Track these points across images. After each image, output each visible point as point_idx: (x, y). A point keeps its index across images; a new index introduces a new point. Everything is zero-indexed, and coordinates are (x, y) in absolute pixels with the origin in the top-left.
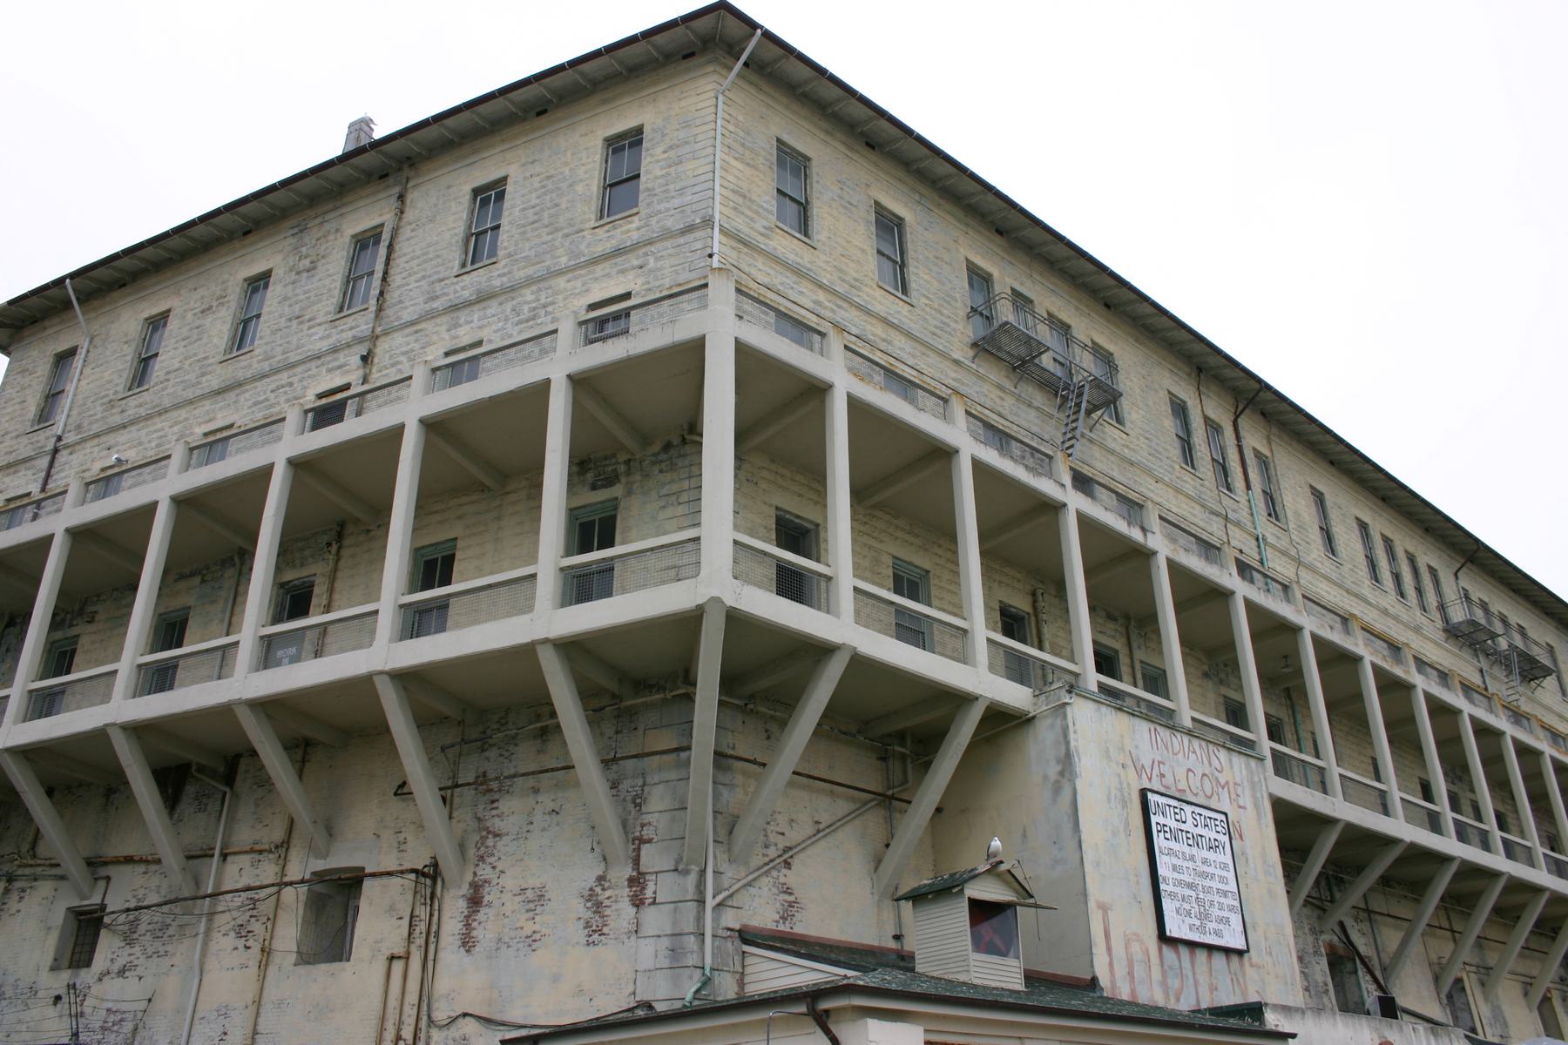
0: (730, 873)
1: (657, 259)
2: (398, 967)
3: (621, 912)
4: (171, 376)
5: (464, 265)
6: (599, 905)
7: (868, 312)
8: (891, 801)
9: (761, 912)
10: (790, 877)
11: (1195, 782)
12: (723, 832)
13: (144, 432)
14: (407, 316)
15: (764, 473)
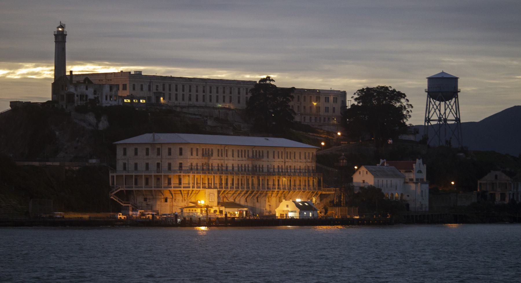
3: (184, 201)
9: (190, 201)
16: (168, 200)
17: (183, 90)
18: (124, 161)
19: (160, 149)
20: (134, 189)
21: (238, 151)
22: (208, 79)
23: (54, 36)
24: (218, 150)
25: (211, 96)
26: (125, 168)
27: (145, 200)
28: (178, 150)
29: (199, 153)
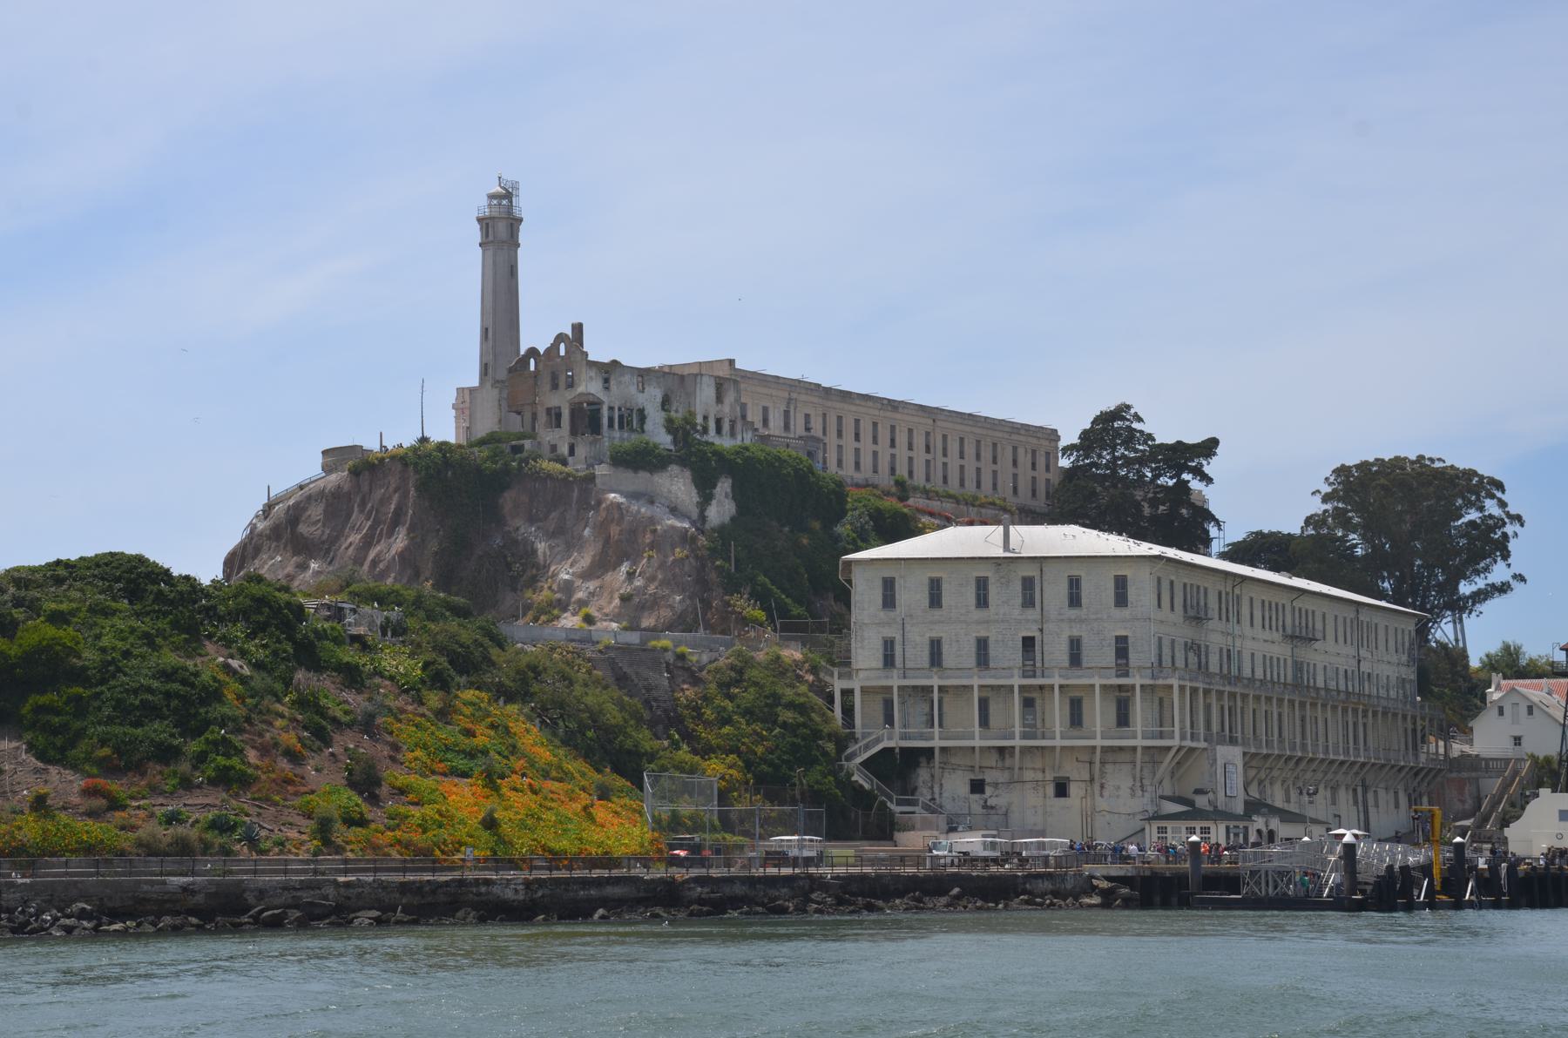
9: (1160, 792)
16: (1074, 789)
17: (875, 441)
18: (889, 632)
19: (1037, 582)
20: (936, 743)
21: (1263, 602)
22: (937, 408)
23: (478, 226)
24: (1220, 593)
25: (945, 464)
26: (889, 661)
27: (977, 787)
28: (1110, 586)
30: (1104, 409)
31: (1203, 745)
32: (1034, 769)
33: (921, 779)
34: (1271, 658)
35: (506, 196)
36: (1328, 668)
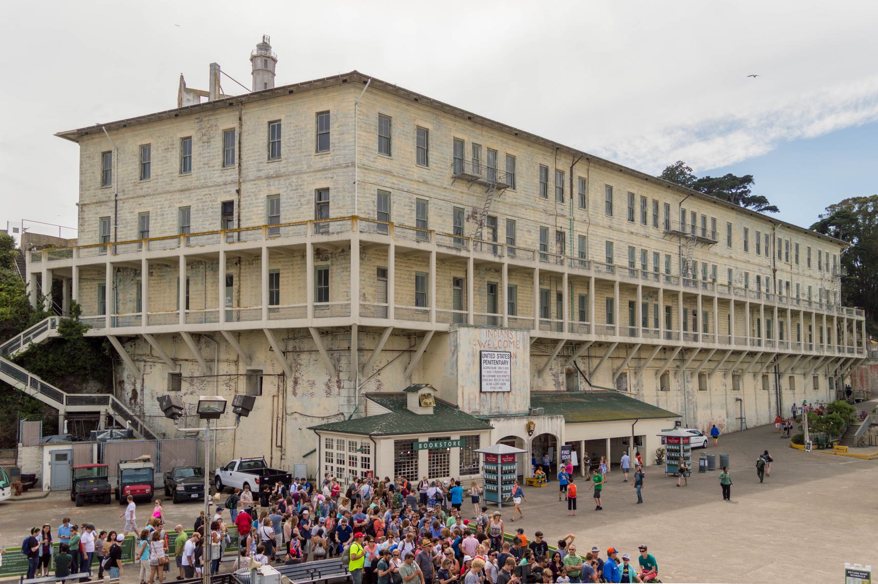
0: (363, 380)
1: (338, 176)
2: (276, 399)
3: (335, 390)
4: (159, 177)
5: (269, 159)
6: (329, 387)
7: (412, 180)
8: (411, 351)
9: (371, 388)
10: (380, 378)
11: (501, 344)
12: (361, 369)
13: (154, 200)
14: (251, 177)
15: (374, 256)
29: (433, 155)
30: (670, 165)
31: (433, 326)
32: (227, 361)
33: (125, 374)
34: (644, 253)
35: (265, 46)
36: (734, 272)
